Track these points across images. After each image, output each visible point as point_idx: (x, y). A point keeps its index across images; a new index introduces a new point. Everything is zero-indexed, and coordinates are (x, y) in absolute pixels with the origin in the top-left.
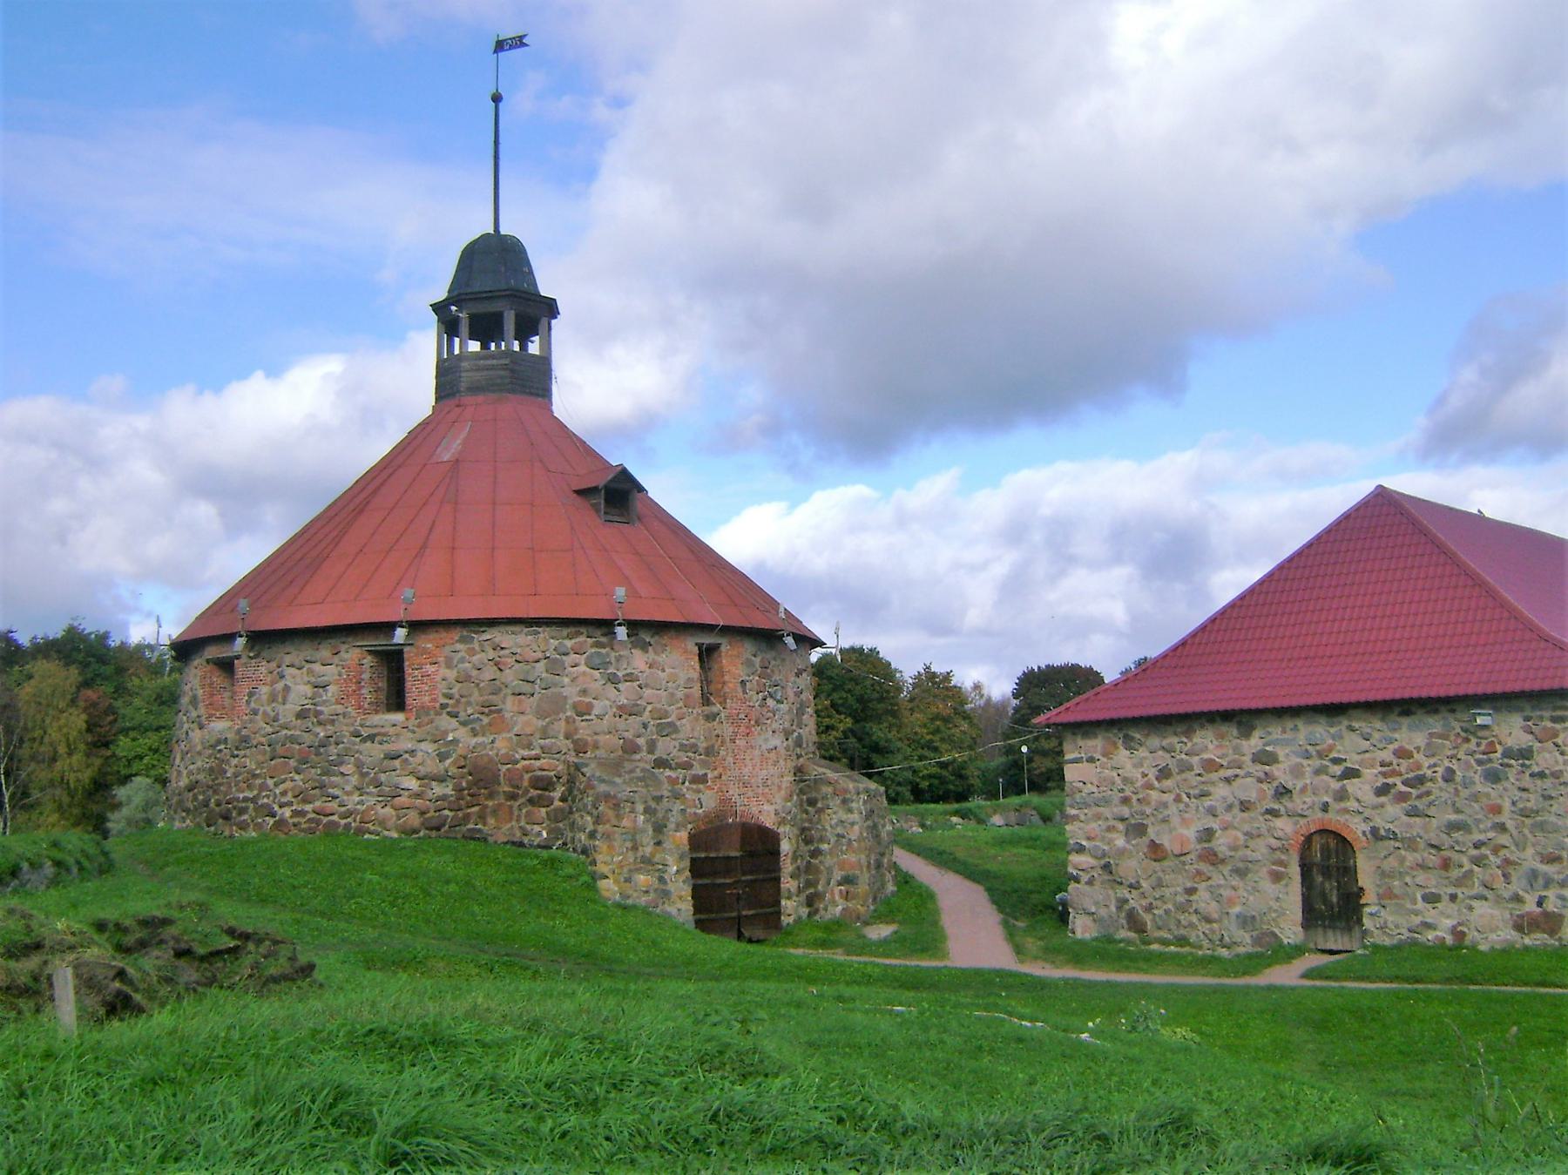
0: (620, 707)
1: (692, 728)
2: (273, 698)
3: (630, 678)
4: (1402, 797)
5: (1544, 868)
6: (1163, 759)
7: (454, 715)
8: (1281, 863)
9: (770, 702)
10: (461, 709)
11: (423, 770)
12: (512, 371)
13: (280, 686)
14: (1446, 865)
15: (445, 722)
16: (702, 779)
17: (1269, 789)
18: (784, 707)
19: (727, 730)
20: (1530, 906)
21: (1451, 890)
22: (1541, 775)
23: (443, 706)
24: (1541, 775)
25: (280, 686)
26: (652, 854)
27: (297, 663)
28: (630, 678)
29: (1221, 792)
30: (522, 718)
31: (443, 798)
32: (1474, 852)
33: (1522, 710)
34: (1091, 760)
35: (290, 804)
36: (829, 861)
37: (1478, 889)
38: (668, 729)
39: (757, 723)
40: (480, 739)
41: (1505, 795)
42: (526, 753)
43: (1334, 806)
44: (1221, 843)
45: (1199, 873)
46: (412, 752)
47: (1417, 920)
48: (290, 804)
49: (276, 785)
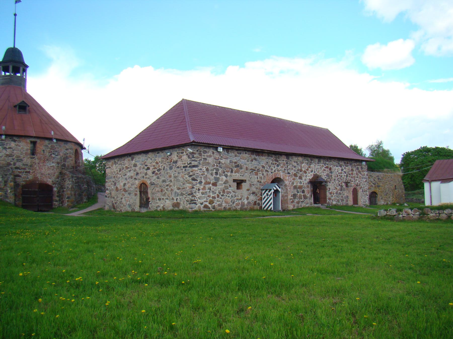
0: (7, 155)
1: (27, 160)
3: (10, 148)
4: (157, 174)
5: (178, 191)
6: (120, 167)
8: (136, 191)
9: (53, 156)
14: (162, 191)
16: (29, 172)
17: (135, 173)
18: (59, 157)
19: (37, 161)
20: (175, 201)
21: (163, 197)
22: (178, 167)
24: (178, 167)
26: (3, 187)
28: (10, 148)
29: (128, 174)
32: (166, 187)
33: (176, 151)
34: (110, 167)
36: (65, 193)
37: (167, 197)
38: (20, 160)
39: (47, 160)
41: (172, 173)
43: (145, 177)
44: (126, 187)
45: (123, 194)
47: (157, 205)
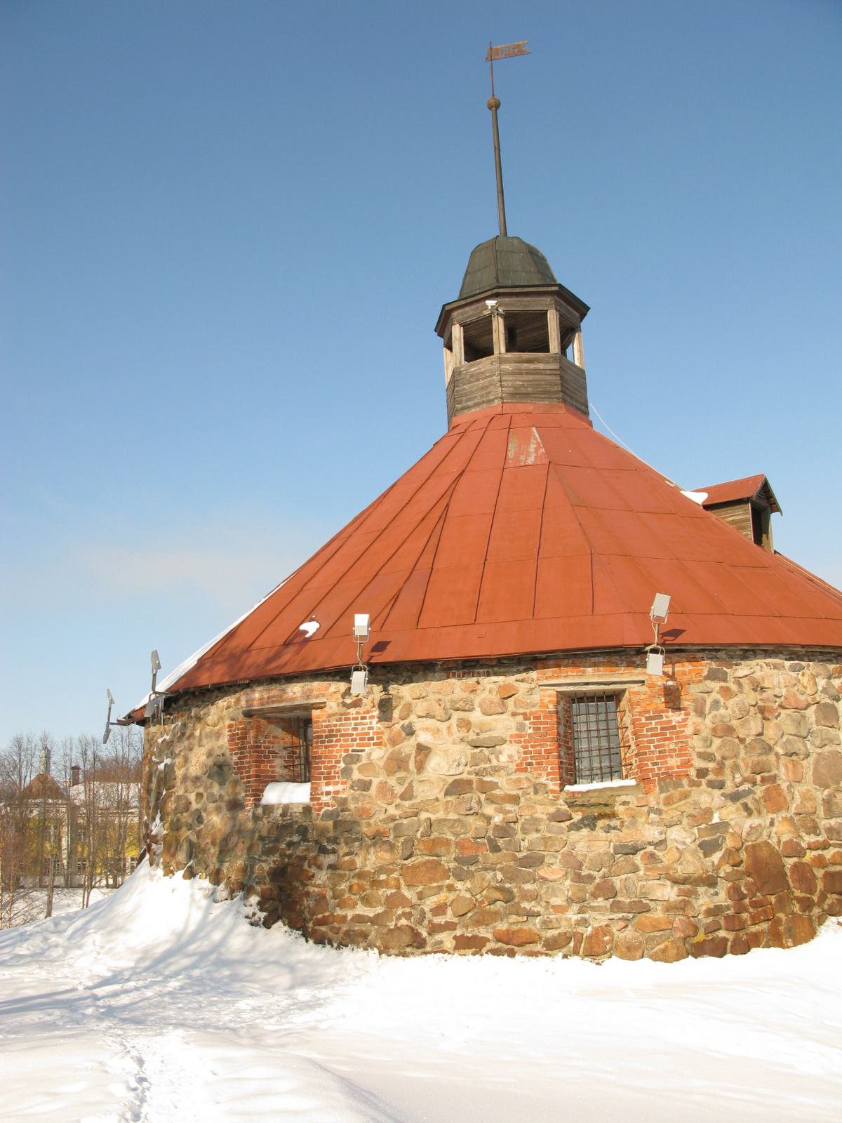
2: (397, 764)
7: (721, 785)
10: (727, 777)
11: (681, 870)
12: (562, 378)
13: (408, 747)
15: (706, 797)
23: (702, 773)
25: (408, 747)
27: (439, 711)
30: (802, 788)
31: (715, 911)
35: (449, 926)
40: (754, 821)
42: (812, 839)
46: (662, 843)
48: (449, 926)
49: (421, 896)
